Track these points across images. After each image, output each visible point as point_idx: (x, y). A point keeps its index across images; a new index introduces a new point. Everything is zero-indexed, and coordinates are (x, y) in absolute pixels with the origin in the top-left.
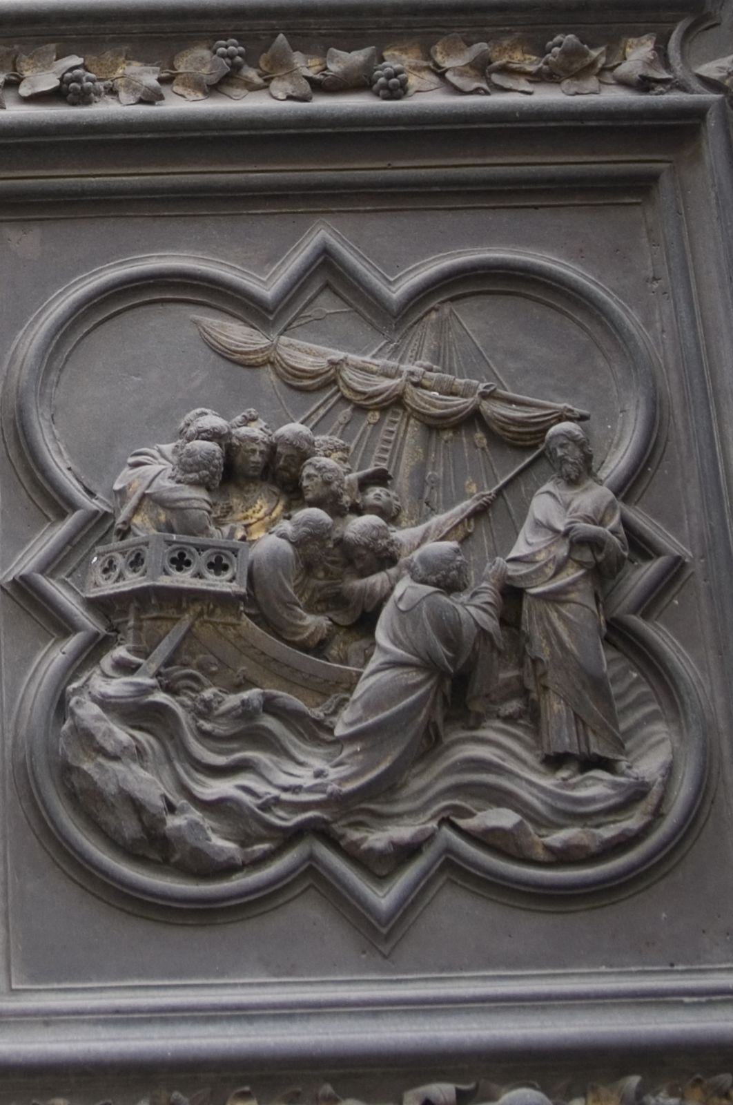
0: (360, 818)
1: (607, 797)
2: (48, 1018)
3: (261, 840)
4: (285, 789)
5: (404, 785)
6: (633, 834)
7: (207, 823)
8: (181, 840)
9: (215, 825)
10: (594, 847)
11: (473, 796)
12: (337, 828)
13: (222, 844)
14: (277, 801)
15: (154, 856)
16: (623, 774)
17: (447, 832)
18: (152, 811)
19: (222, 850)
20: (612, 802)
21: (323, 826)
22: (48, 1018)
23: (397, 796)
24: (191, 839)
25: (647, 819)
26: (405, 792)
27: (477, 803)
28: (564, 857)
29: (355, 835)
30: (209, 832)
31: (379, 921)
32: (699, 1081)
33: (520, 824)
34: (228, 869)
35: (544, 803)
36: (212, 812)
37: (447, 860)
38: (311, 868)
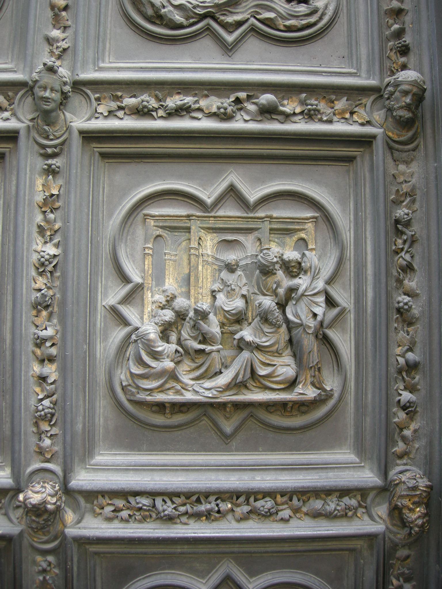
0: (224, 12)
1: (305, 11)
2: (119, 69)
3: (193, 18)
4: (201, 3)
5: (240, 4)
6: (311, 23)
7: (175, 12)
8: (166, 16)
9: (177, 12)
10: (299, 26)
11: (262, 8)
12: (217, 15)
13: (178, 18)
14: (198, 6)
15: (158, 22)
16: (311, 5)
17: (253, 20)
18: (157, 6)
19: (179, 20)
20: (306, 13)
21: (213, 14)
22: (119, 69)
23: (237, 7)
24: (169, 16)
25: (317, 19)
26: (241, 6)
27: (263, 11)
28: (289, 29)
29: (222, 18)
30: (176, 15)
31: (228, 45)
32: (325, 97)
33: (276, 17)
34: (181, 27)
35: (285, 12)
36: (178, 9)
37: (252, 28)
38: (208, 29)
